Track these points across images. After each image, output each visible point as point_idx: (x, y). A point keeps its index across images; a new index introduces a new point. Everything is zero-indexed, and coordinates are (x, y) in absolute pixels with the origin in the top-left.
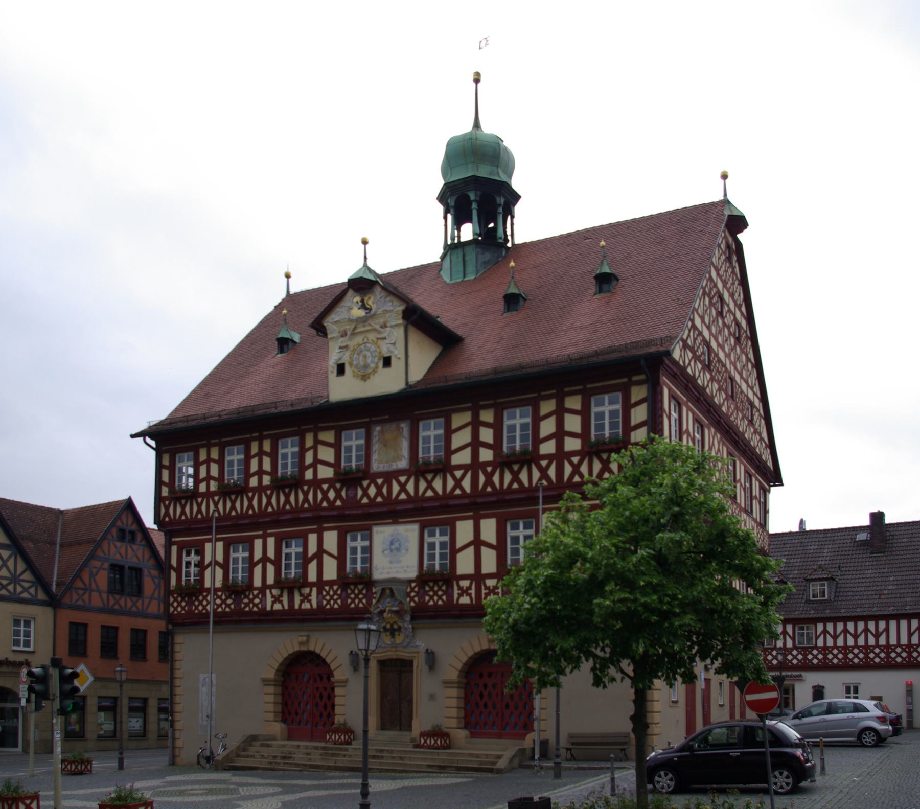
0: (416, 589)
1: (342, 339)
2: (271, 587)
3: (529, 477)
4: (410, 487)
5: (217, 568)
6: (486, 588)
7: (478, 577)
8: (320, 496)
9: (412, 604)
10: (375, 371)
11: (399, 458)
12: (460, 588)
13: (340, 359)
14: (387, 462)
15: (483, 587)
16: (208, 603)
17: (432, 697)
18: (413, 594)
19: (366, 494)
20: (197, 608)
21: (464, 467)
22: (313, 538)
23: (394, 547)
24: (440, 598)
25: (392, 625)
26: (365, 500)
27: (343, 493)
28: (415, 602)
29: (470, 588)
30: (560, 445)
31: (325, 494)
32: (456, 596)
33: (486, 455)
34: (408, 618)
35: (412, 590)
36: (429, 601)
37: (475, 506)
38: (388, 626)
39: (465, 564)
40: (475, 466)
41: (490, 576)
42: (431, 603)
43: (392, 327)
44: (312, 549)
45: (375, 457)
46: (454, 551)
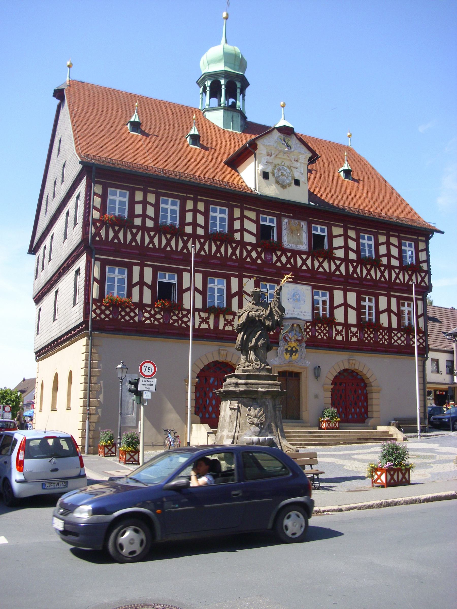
0: (310, 327)
1: (267, 157)
2: (199, 311)
3: (375, 274)
4: (309, 262)
5: (145, 288)
6: (351, 332)
7: (346, 325)
8: (245, 254)
9: (308, 336)
10: (289, 185)
11: (302, 243)
12: (336, 330)
13: (266, 169)
14: (293, 243)
15: (349, 332)
16: (136, 315)
17: (316, 396)
18: (308, 330)
19: (279, 259)
20: (123, 317)
21: (342, 260)
22: (235, 282)
23: (296, 298)
24: (325, 334)
25: (292, 349)
26: (279, 264)
27: (263, 255)
28: (309, 335)
29: (342, 331)
30: (389, 261)
31: (249, 253)
32: (334, 335)
33: (353, 256)
34: (304, 345)
35: (308, 327)
36: (318, 336)
37: (347, 283)
38: (289, 349)
39: (339, 315)
40: (346, 260)
41: (353, 326)
42: (320, 337)
43: (300, 163)
44: (235, 288)
45: (285, 238)
46: (333, 308)
